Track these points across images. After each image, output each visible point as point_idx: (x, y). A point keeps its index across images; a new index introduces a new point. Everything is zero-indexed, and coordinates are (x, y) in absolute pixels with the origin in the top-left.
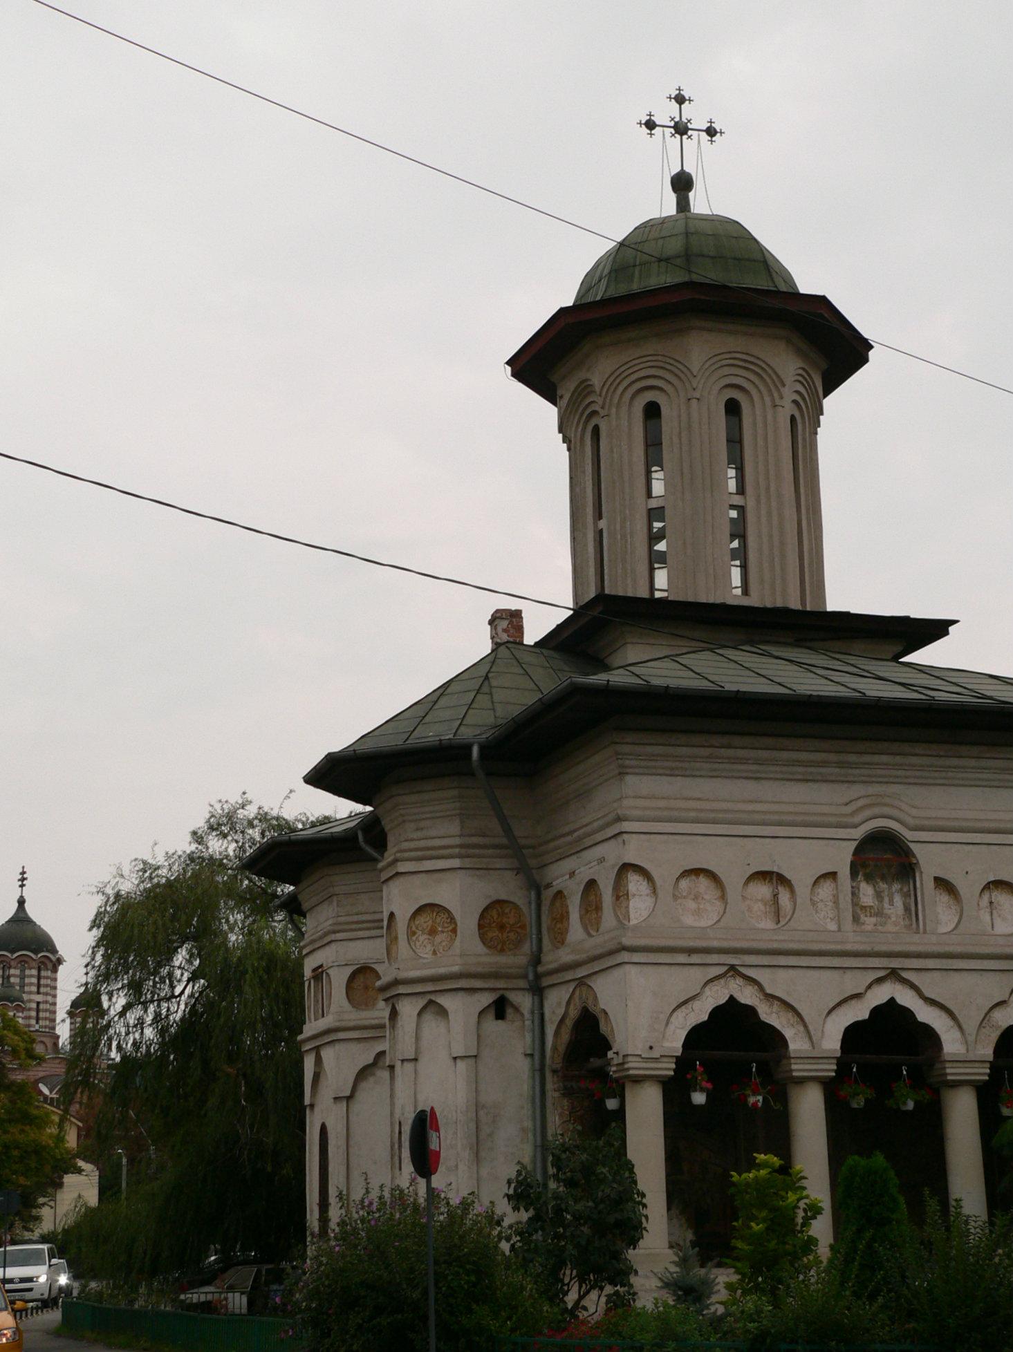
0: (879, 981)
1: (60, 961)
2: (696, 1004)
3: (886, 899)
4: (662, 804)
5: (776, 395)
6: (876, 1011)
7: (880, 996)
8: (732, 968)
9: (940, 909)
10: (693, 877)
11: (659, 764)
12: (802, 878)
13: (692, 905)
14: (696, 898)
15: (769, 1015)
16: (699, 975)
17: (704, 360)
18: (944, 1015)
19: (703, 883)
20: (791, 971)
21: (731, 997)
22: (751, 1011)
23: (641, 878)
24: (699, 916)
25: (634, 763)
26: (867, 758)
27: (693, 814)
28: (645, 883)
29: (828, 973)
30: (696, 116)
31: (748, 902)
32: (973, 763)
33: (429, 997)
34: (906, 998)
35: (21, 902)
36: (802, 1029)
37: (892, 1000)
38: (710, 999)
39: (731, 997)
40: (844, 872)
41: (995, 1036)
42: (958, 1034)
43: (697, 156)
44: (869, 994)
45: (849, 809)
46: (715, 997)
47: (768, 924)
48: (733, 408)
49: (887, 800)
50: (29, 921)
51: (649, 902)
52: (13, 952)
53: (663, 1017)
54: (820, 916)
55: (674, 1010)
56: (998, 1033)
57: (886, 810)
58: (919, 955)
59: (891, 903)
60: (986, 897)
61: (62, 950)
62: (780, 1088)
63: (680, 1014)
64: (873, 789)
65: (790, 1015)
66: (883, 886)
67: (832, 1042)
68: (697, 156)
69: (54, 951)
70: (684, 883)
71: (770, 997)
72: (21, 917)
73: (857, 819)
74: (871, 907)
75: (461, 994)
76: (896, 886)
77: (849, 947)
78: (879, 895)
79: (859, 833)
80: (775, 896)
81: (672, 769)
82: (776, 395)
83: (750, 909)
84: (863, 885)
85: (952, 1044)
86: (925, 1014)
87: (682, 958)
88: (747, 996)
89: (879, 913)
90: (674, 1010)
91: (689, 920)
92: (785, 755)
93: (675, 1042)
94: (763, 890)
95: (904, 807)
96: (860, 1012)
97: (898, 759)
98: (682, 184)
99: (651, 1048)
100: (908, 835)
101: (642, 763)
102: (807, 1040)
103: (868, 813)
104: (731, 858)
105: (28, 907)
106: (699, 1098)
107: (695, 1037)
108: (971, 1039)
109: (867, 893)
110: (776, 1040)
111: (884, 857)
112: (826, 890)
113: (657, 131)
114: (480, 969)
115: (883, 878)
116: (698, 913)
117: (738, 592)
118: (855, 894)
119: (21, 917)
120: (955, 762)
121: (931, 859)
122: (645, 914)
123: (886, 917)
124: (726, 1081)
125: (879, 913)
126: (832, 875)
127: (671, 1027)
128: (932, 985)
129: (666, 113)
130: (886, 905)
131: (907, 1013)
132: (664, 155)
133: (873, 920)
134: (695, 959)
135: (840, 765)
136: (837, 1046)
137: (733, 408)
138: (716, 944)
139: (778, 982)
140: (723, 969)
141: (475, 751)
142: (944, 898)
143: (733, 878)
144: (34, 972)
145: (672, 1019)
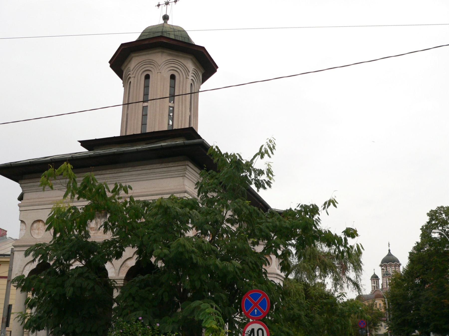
4: (32, 201)
11: (33, 189)
13: (37, 231)
14: (38, 229)
17: (162, 65)
32: (127, 174)
35: (389, 251)
42: (113, 270)
50: (392, 255)
52: (388, 263)
53: (23, 267)
56: (128, 269)
61: (401, 262)
63: (28, 266)
69: (398, 262)
70: (35, 225)
72: (390, 254)
74: (94, 228)
81: (36, 189)
91: (35, 236)
98: (166, 18)
101: (28, 189)
105: (391, 251)
108: (117, 271)
113: (160, 6)
115: (99, 217)
116: (38, 234)
119: (390, 254)
120: (121, 174)
133: (94, 232)
137: (147, 77)
144: (394, 268)
145: (26, 268)
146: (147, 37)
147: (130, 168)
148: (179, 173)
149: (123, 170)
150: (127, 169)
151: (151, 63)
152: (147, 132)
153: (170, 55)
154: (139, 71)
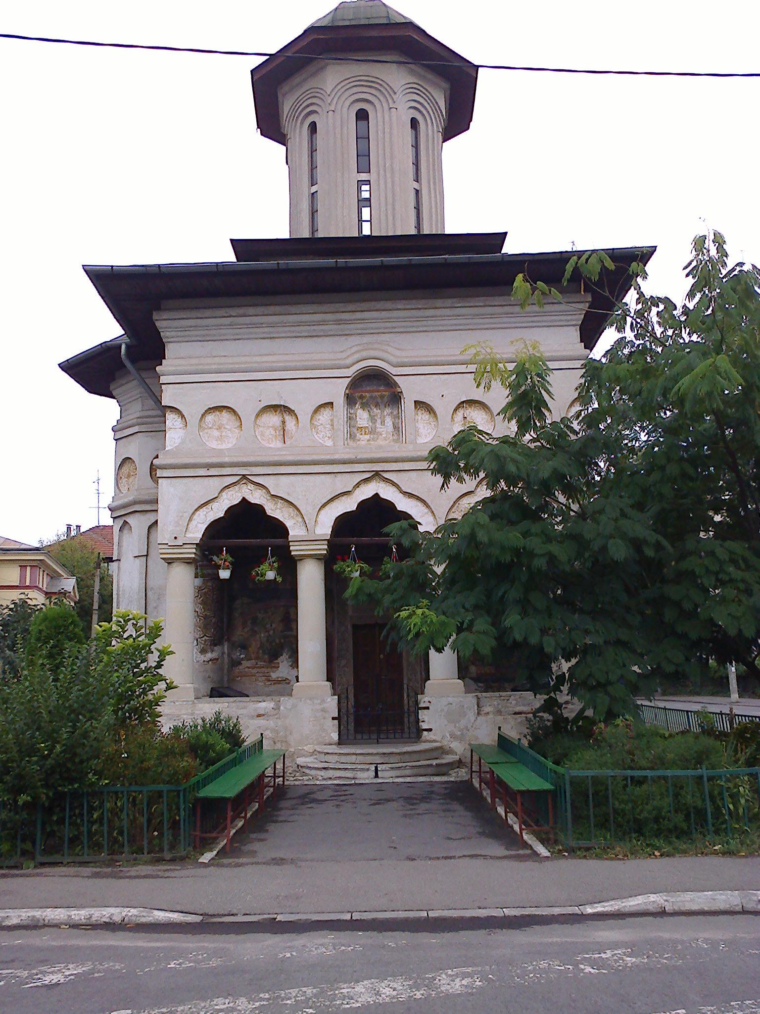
0: (366, 480)
2: (215, 505)
3: (379, 421)
4: (193, 361)
5: (390, 101)
6: (362, 504)
7: (366, 492)
8: (244, 476)
9: (420, 425)
10: (218, 413)
12: (304, 409)
13: (216, 433)
14: (219, 428)
15: (273, 510)
16: (216, 484)
18: (419, 504)
19: (225, 415)
20: (291, 477)
21: (244, 498)
22: (260, 509)
23: (176, 416)
24: (223, 441)
25: (173, 334)
26: (358, 315)
27: (214, 367)
28: (180, 419)
29: (323, 476)
31: (261, 429)
32: (447, 312)
33: (124, 518)
36: (301, 520)
37: (377, 495)
38: (226, 501)
39: (244, 498)
40: (340, 402)
42: (431, 518)
44: (357, 491)
45: (344, 355)
46: (232, 498)
47: (279, 444)
48: (362, 116)
49: (376, 346)
51: (181, 433)
53: (187, 516)
54: (324, 436)
55: (196, 510)
57: (372, 353)
58: (396, 460)
59: (383, 423)
60: (460, 414)
62: (289, 565)
63: (201, 512)
64: (366, 339)
65: (291, 509)
66: (376, 411)
67: (325, 527)
70: (209, 418)
73: (348, 361)
75: (137, 515)
76: (388, 411)
77: (336, 457)
78: (372, 419)
79: (351, 372)
80: (284, 422)
82: (390, 101)
83: (262, 435)
84: (360, 411)
87: (202, 472)
88: (256, 497)
89: (373, 431)
90: (196, 510)
91: (214, 444)
92: (291, 318)
93: (197, 533)
94: (274, 419)
95: (390, 349)
96: (349, 505)
97: (384, 314)
99: (176, 538)
100: (393, 371)
102: (304, 528)
103: (357, 357)
104: (246, 397)
106: (225, 574)
107: (215, 529)
109: (362, 417)
110: (281, 530)
111: (373, 387)
112: (325, 416)
114: (147, 497)
115: (377, 405)
116: (220, 439)
118: (351, 418)
120: (432, 312)
121: (411, 389)
122: (178, 441)
123: (377, 435)
124: (244, 563)
125: (373, 431)
127: (193, 523)
130: (378, 425)
133: (367, 437)
134: (213, 472)
135: (339, 322)
136: (329, 531)
137: (362, 116)
138: (227, 460)
139: (280, 486)
140: (239, 478)
141: (123, 347)
143: (247, 412)
145: (195, 517)
146: (353, 23)
147: (455, 300)
148: (569, 318)
149: (439, 303)
150: (449, 302)
151: (373, 84)
152: (452, 227)
153: (412, 72)
154: (343, 99)
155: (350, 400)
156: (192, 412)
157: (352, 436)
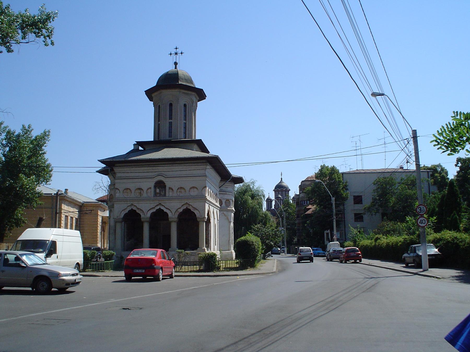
0: (158, 205)
1: (289, 190)
7: (158, 208)
12: (145, 190)
13: (126, 194)
19: (129, 190)
22: (135, 211)
30: (179, 51)
34: (162, 208)
35: (282, 179)
41: (178, 213)
43: (179, 59)
46: (129, 209)
67: (149, 215)
68: (179, 59)
71: (138, 209)
85: (170, 215)
86: (165, 210)
93: (122, 215)
94: (139, 191)
98: (176, 64)
107: (126, 215)
111: (160, 185)
112: (149, 190)
117: (183, 135)
126: (150, 188)
128: (167, 205)
129: (173, 51)
131: (163, 210)
132: (174, 58)
142: (171, 190)
155: (155, 187)
156: (121, 190)
157: (156, 195)
